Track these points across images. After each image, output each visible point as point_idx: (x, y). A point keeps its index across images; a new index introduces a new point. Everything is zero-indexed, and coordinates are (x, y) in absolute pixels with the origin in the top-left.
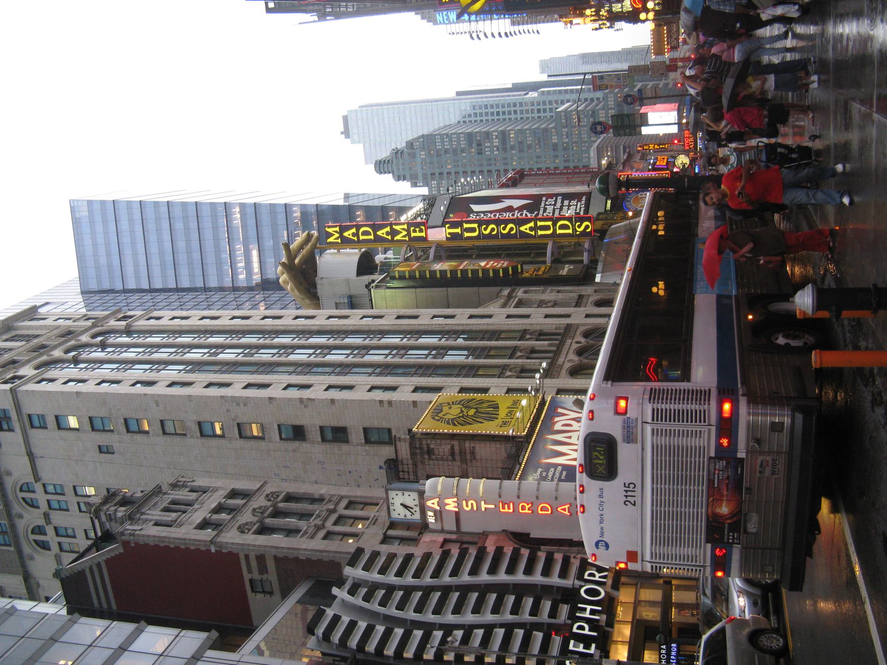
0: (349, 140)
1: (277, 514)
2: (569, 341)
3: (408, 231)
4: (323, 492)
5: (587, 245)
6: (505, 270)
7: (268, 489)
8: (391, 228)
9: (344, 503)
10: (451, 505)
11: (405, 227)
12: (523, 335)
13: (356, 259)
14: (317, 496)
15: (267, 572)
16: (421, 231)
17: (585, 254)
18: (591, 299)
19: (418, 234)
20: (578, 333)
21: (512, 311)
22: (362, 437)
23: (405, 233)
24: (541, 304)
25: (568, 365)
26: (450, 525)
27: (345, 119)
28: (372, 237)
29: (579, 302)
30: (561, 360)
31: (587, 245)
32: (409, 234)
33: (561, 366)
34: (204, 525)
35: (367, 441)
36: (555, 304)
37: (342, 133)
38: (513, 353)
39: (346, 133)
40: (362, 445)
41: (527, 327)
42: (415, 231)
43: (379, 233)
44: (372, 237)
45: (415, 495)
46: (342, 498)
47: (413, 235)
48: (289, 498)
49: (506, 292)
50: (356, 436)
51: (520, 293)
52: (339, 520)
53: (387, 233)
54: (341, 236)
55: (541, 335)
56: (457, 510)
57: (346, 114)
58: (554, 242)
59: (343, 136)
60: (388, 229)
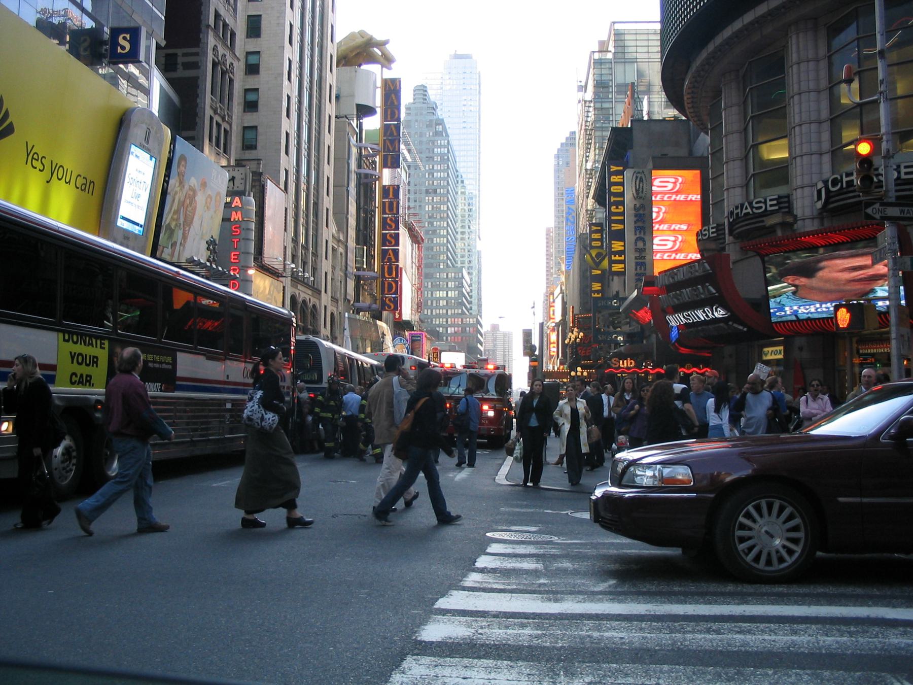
1: (224, 73)
2: (310, 292)
7: (235, 64)
12: (315, 254)
15: (184, 69)
24: (333, 267)
25: (297, 292)
29: (334, 299)
30: (300, 287)
33: (296, 288)
34: (217, 15)
38: (305, 248)
41: (319, 258)
48: (231, 81)
52: (218, 125)
55: (314, 269)
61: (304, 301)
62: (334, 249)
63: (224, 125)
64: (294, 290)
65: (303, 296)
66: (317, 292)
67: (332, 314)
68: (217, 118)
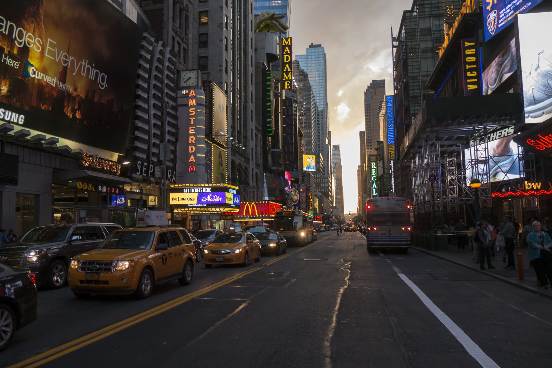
0: (308, 47)
1: (181, 10)
3: (288, 80)
4: (190, 35)
5: (280, 169)
6: (270, 127)
7: (190, 6)
8: (290, 72)
9: (185, 46)
10: (193, 102)
11: (290, 79)
13: (274, 53)
14: (188, 32)
16: (288, 87)
17: (276, 168)
18: (258, 170)
19: (286, 85)
20: (246, 164)
21: (254, 132)
22: (203, 55)
23: (287, 78)
24: (256, 146)
25: (235, 159)
26: (180, 101)
27: (320, 46)
28: (285, 61)
29: (257, 165)
30: (237, 156)
31: (280, 169)
32: (286, 80)
33: (235, 156)
35: (200, 58)
36: (256, 153)
37: (312, 44)
39: (312, 46)
40: (198, 55)
42: (288, 83)
43: (287, 65)
44: (285, 61)
45: (195, 84)
46: (187, 45)
47: (286, 82)
48: (187, 17)
49: (260, 128)
50: (203, 52)
51: (260, 136)
53: (287, 69)
54: (286, 46)
56: (190, 105)
57: (322, 46)
58: (281, 153)
59: (311, 44)
60: (289, 70)
61: (240, 165)
62: (256, 135)
63: (183, 45)
64: (233, 157)
65: (239, 161)
66: (247, 160)
67: (256, 173)
68: (177, 39)
